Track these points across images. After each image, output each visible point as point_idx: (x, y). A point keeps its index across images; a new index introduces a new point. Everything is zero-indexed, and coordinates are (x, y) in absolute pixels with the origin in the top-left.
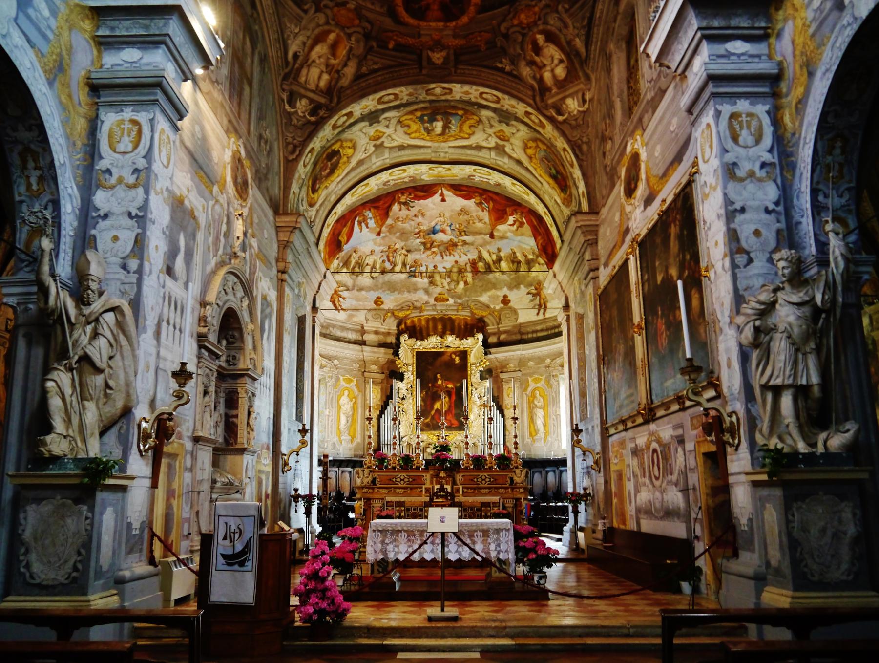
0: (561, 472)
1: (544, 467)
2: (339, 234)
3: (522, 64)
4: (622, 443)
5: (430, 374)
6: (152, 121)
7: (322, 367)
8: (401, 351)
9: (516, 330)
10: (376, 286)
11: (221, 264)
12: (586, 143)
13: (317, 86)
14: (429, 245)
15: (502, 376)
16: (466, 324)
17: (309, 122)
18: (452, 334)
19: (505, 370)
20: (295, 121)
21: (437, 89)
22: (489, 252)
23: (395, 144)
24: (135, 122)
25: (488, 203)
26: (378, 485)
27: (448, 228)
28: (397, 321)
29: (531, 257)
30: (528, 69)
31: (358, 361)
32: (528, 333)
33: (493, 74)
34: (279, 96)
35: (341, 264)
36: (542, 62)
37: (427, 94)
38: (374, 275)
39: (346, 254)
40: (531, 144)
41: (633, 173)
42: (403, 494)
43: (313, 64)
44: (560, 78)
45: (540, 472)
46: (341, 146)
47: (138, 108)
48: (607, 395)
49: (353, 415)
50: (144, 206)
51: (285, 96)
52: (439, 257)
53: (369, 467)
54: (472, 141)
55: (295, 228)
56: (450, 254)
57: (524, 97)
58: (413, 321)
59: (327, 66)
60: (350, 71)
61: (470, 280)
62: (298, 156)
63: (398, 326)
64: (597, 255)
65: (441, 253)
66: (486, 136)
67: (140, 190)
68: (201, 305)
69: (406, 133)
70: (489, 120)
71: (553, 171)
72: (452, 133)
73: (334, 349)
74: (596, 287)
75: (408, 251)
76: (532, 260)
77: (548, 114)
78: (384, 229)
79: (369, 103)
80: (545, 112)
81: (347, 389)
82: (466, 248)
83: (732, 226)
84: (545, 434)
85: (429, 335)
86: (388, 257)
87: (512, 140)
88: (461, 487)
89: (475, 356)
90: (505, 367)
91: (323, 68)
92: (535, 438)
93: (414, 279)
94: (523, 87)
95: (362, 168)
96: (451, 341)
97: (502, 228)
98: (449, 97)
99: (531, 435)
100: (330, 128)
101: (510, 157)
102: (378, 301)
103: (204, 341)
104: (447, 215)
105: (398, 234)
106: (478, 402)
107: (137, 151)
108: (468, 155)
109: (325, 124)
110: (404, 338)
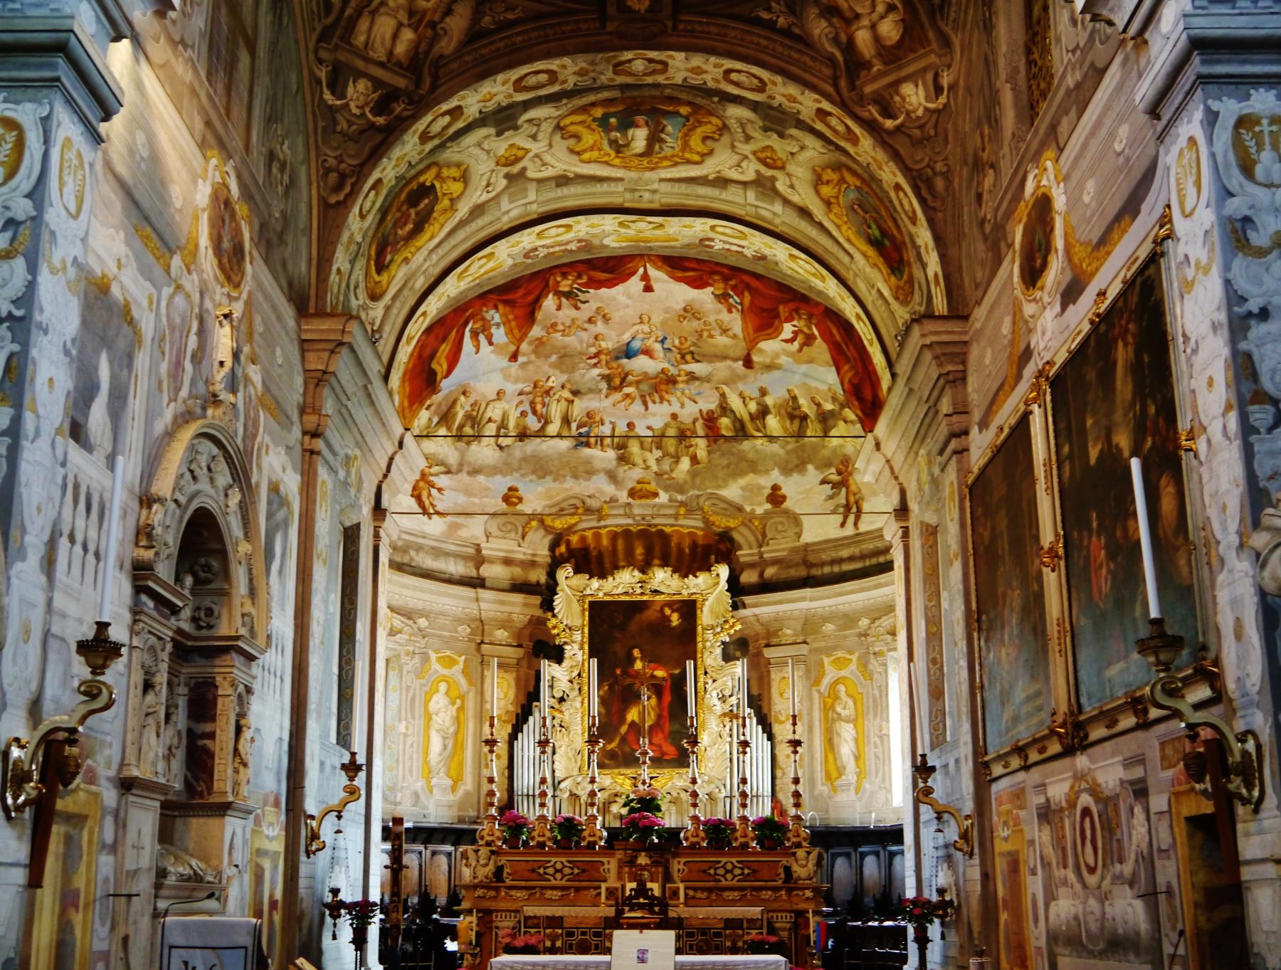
0: (892, 855)
1: (856, 846)
2: (432, 356)
3: (812, 12)
4: (1018, 795)
5: (618, 648)
6: (46, 121)
7: (392, 633)
8: (558, 601)
9: (798, 558)
10: (507, 464)
11: (185, 417)
12: (942, 174)
13: (390, 53)
14: (617, 381)
15: (768, 653)
16: (694, 545)
17: (372, 126)
18: (664, 564)
19: (775, 641)
20: (343, 125)
21: (637, 61)
22: (741, 395)
23: (549, 172)
24: (11, 124)
25: (740, 294)
26: (508, 882)
27: (658, 346)
28: (550, 537)
29: (828, 406)
30: (824, 24)
31: (469, 621)
32: (823, 564)
33: (750, 33)
34: (311, 73)
35: (436, 420)
36: (851, 9)
37: (615, 72)
38: (504, 442)
39: (446, 397)
40: (829, 175)
41: (1039, 235)
42: (562, 901)
43: (382, 10)
44: (889, 43)
45: (848, 855)
46: (438, 176)
47: (18, 94)
48: (986, 694)
49: (457, 733)
50: (27, 298)
51: (322, 74)
52: (637, 407)
53: (488, 844)
54: (708, 168)
55: (341, 344)
56: (662, 399)
57: (815, 80)
58: (583, 539)
59: (411, 12)
60: (457, 24)
61: (702, 453)
62: (348, 196)
63: (553, 547)
64: (965, 403)
65: (643, 397)
66: (736, 158)
67: (19, 264)
68: (141, 502)
69: (572, 151)
70: (742, 126)
71: (875, 232)
72: (668, 152)
73: (418, 594)
74: (963, 471)
75: (576, 393)
76: (832, 412)
77: (865, 115)
78: (524, 346)
79: (497, 90)
80: (858, 110)
81: (444, 679)
83: (1243, 346)
84: (859, 775)
85: (616, 567)
87: (791, 168)
88: (682, 886)
89: (711, 611)
90: (775, 634)
91: (403, 17)
92: (837, 783)
93: (587, 451)
94: (814, 59)
95: (480, 222)
96: (663, 579)
97: (769, 347)
98: (660, 79)
99: (828, 777)
100: (416, 139)
101: (786, 202)
102: (511, 497)
103: (148, 578)
104: (656, 319)
105: (554, 358)
106: (719, 708)
107: (13, 183)
108: (698, 196)
109: (405, 131)
110: (565, 574)
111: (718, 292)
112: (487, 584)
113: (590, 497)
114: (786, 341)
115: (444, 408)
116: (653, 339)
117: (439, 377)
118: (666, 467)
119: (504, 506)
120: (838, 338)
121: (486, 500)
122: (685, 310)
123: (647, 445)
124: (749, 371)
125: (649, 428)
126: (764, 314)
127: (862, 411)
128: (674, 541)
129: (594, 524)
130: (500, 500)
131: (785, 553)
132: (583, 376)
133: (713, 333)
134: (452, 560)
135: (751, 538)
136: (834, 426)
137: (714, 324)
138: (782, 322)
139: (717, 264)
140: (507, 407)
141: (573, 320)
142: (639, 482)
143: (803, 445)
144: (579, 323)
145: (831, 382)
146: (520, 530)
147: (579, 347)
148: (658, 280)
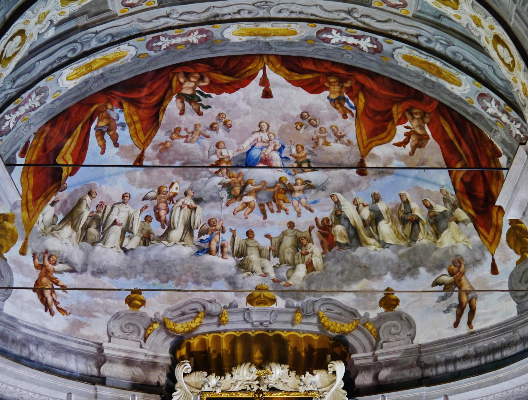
2: (57, 151)
9: (411, 360)
14: (237, 190)
16: (310, 349)
18: (281, 361)
25: (354, 97)
27: (276, 156)
28: (171, 340)
29: (440, 208)
32: (437, 365)
35: (61, 217)
38: (129, 244)
39: (71, 196)
52: (256, 216)
56: (280, 208)
58: (203, 342)
61: (317, 261)
63: (174, 350)
65: (261, 205)
73: (34, 388)
75: (198, 201)
76: (443, 213)
78: (149, 151)
82: (311, 195)
86: (156, 209)
93: (208, 258)
104: (275, 128)
111: (333, 97)
112: (108, 382)
113: (210, 302)
114: (399, 145)
115: (70, 207)
116: (271, 148)
117: (64, 173)
118: (284, 275)
119: (127, 307)
120: (451, 135)
121: (110, 301)
122: (302, 116)
123: (265, 253)
124: (364, 177)
125: (268, 236)
126: (378, 118)
127: (474, 209)
128: (291, 345)
129: (215, 328)
130: (124, 302)
131: (399, 355)
132: (206, 183)
133: (328, 140)
134: (73, 357)
135: (366, 342)
136: (446, 228)
137: (329, 131)
138: (395, 125)
139: (334, 63)
140: (132, 211)
141: (196, 126)
142: (258, 289)
143: (415, 249)
144: (201, 129)
145: (443, 183)
146: (142, 332)
147: (201, 154)
148: (276, 84)
